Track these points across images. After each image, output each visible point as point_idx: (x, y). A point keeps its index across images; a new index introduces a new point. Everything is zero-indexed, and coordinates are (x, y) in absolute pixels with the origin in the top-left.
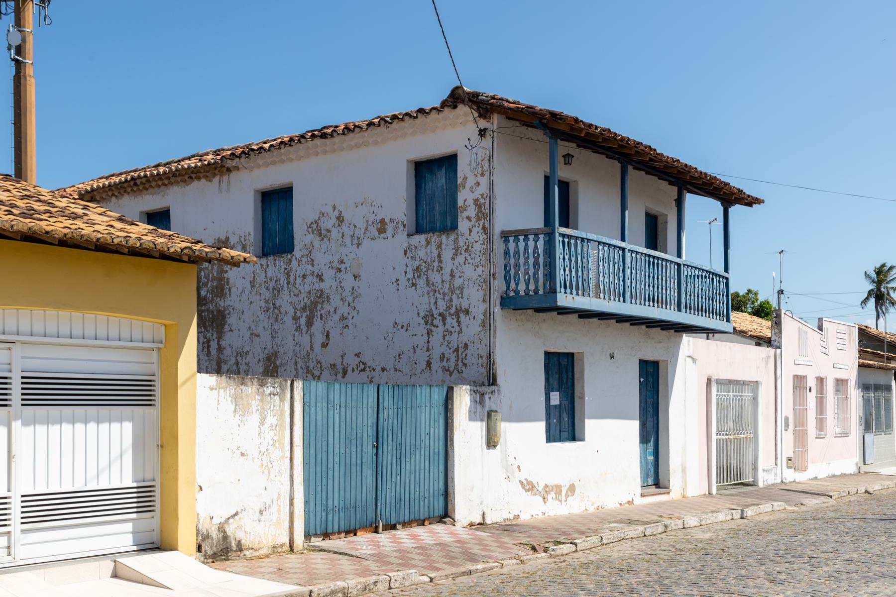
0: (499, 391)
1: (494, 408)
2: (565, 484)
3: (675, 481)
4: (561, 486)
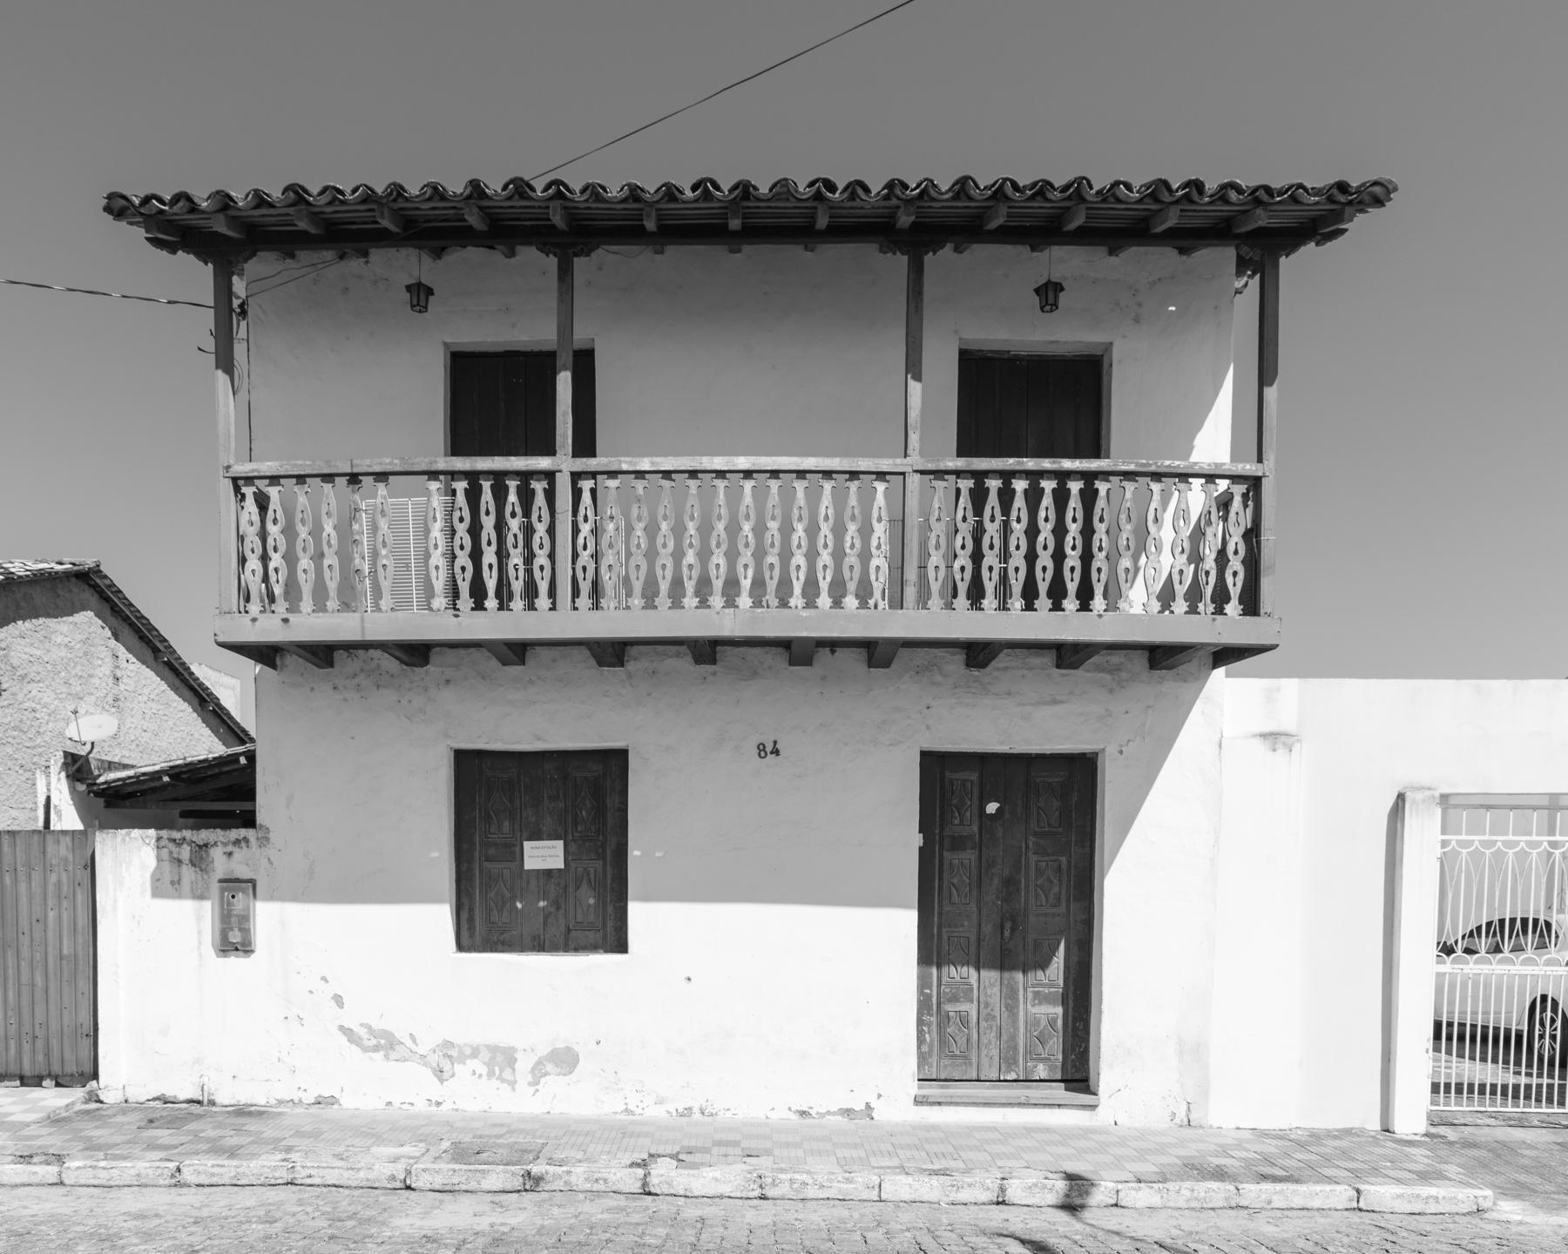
0: (264, 841)
1: (243, 872)
2: (532, 1041)
3: (1109, 1070)
4: (513, 1050)
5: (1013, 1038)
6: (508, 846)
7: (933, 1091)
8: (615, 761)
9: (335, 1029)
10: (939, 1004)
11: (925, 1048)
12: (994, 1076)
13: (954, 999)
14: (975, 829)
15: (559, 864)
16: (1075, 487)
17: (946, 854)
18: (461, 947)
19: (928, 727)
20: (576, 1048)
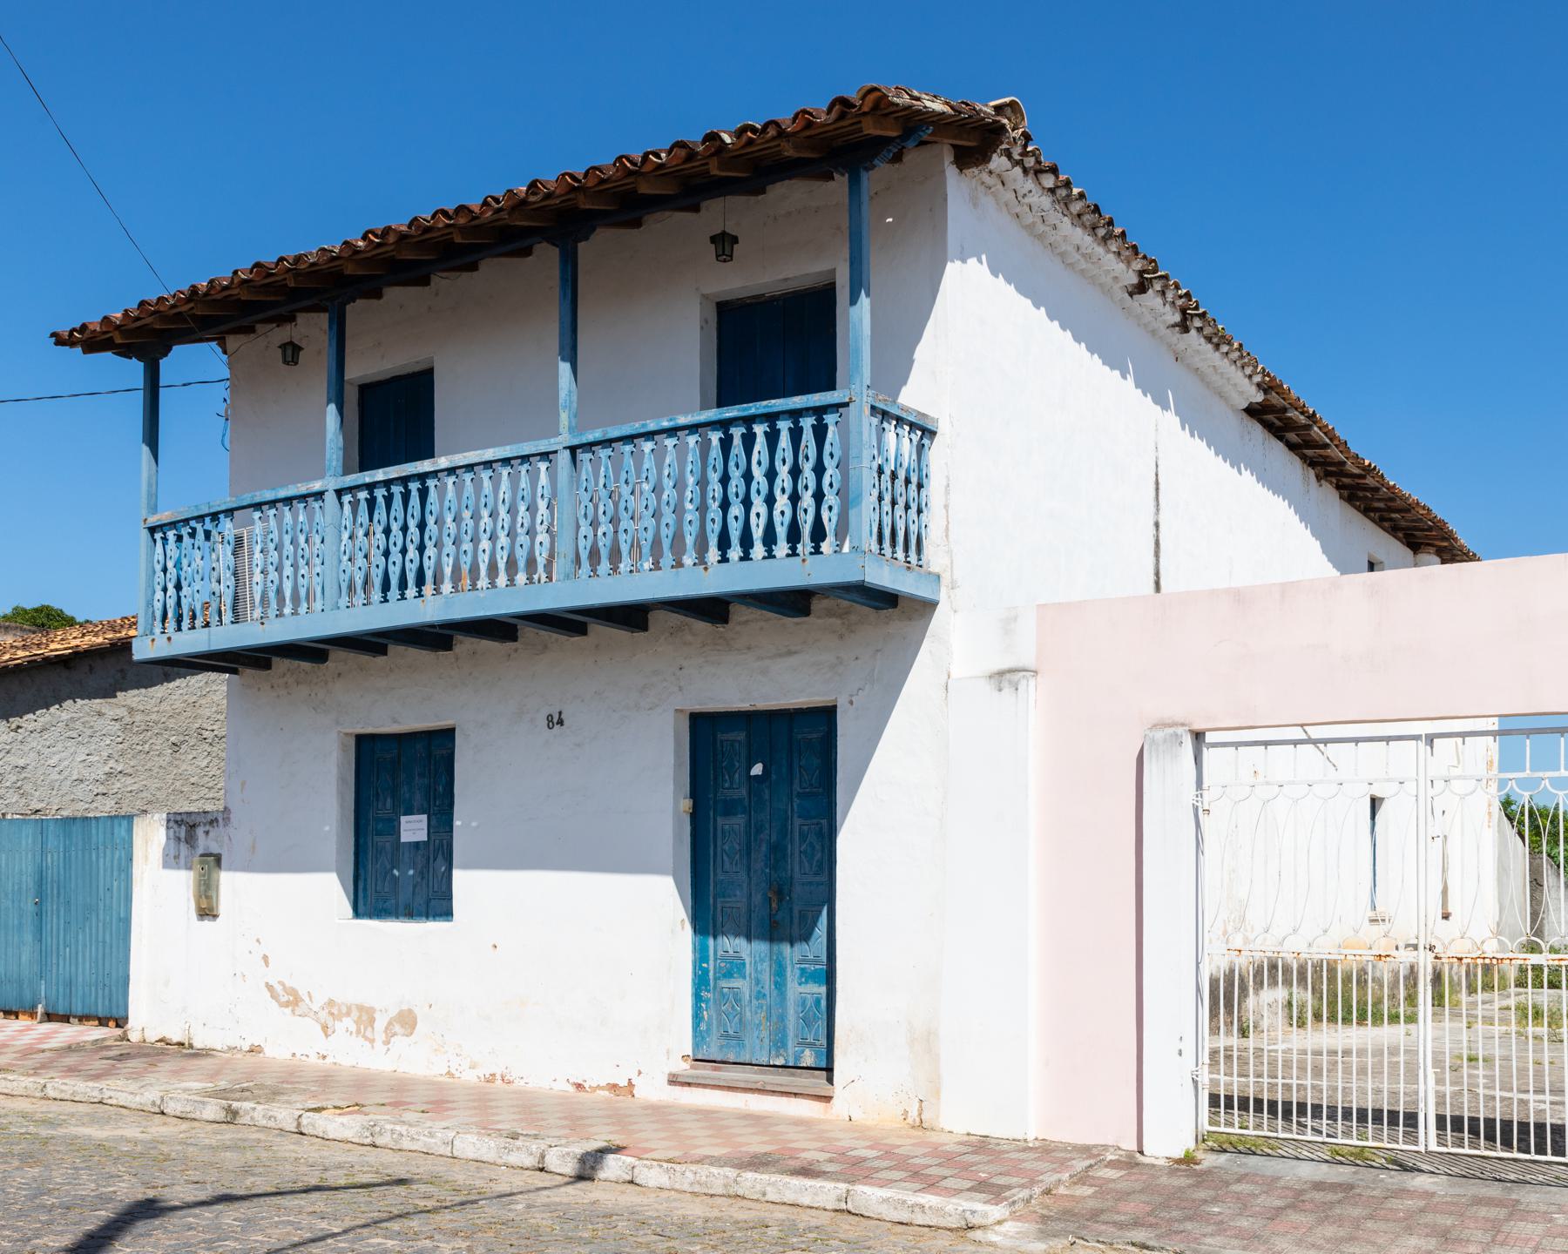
1: (215, 849)
2: (386, 1005)
5: (782, 1018)
6: (390, 820)
7: (706, 1072)
8: (446, 736)
9: (263, 985)
10: (715, 979)
11: (703, 1027)
12: (764, 1060)
13: (728, 975)
14: (744, 792)
15: (422, 836)
16: (807, 423)
17: (719, 819)
18: (357, 913)
19: (681, 689)
20: (416, 1011)
